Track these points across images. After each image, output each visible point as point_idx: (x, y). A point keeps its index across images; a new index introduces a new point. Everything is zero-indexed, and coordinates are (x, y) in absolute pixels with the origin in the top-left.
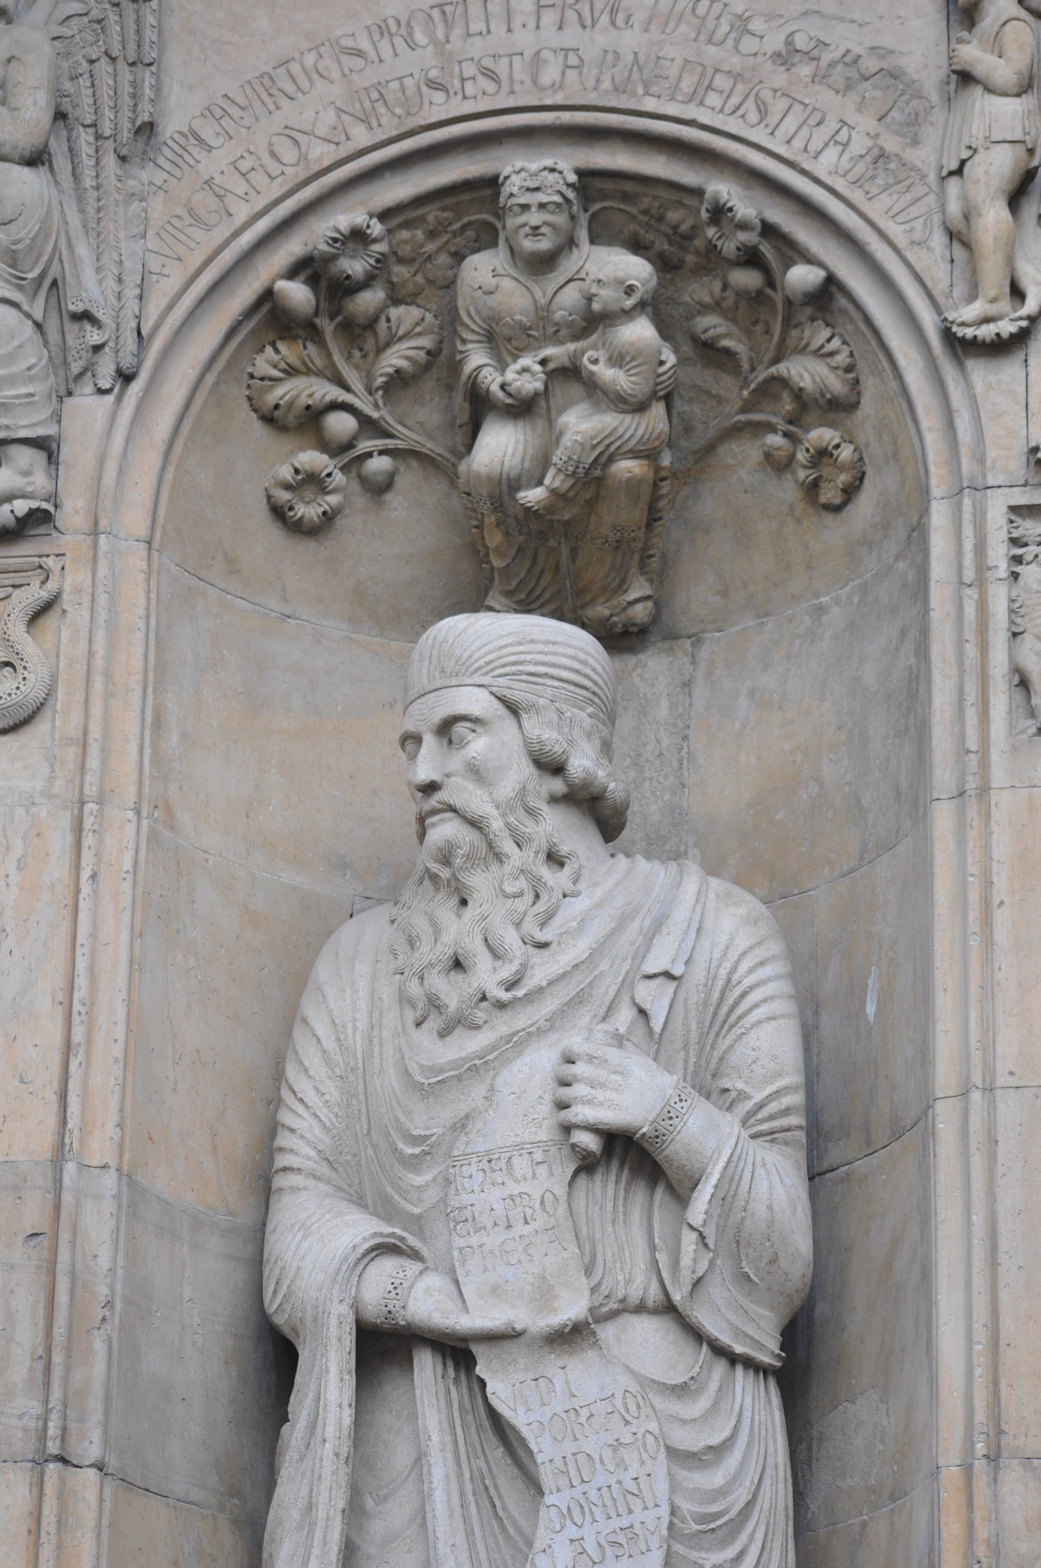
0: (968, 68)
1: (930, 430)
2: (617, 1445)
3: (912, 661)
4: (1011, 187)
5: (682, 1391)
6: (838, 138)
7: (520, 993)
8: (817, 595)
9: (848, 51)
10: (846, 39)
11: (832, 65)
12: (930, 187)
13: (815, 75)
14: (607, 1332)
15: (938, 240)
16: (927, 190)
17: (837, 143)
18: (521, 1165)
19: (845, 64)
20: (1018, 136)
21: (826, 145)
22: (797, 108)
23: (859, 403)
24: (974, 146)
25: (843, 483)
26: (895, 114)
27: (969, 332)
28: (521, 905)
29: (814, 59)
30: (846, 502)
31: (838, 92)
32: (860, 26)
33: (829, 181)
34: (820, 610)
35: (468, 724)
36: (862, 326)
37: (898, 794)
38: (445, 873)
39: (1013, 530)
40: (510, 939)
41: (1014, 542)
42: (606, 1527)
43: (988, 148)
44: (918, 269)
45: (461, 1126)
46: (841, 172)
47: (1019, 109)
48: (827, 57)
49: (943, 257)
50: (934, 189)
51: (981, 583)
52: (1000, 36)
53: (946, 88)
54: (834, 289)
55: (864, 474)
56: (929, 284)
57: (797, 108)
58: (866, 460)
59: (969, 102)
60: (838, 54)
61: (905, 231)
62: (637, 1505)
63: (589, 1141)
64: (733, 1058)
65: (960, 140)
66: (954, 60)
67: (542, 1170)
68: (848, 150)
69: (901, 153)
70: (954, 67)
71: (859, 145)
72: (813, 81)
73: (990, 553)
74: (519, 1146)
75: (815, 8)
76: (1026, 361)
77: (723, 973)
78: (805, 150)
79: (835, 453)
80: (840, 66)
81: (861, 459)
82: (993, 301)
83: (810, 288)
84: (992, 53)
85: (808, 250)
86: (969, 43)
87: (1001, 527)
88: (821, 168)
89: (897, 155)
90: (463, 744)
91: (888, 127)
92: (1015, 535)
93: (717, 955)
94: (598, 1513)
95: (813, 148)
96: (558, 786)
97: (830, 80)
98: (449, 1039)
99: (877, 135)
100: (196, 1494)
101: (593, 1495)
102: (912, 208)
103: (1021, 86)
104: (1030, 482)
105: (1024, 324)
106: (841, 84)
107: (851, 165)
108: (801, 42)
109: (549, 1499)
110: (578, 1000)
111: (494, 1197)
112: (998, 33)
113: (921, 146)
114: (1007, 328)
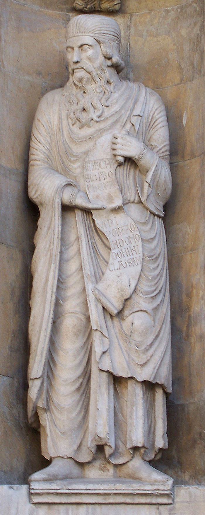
2: (129, 238)
3: (198, 32)
5: (145, 223)
7: (102, 119)
8: (167, 7)
14: (125, 207)
18: (103, 164)
28: (101, 95)
34: (168, 11)
35: (88, 46)
38: (80, 85)
40: (99, 105)
42: (127, 258)
45: (87, 153)
62: (134, 253)
63: (121, 159)
64: (154, 137)
67: (108, 166)
74: (103, 159)
77: (151, 114)
90: (86, 51)
93: (150, 110)
94: (125, 254)
96: (109, 63)
98: (82, 129)
100: (12, 244)
101: (124, 250)
109: (112, 251)
110: (117, 121)
111: (96, 172)
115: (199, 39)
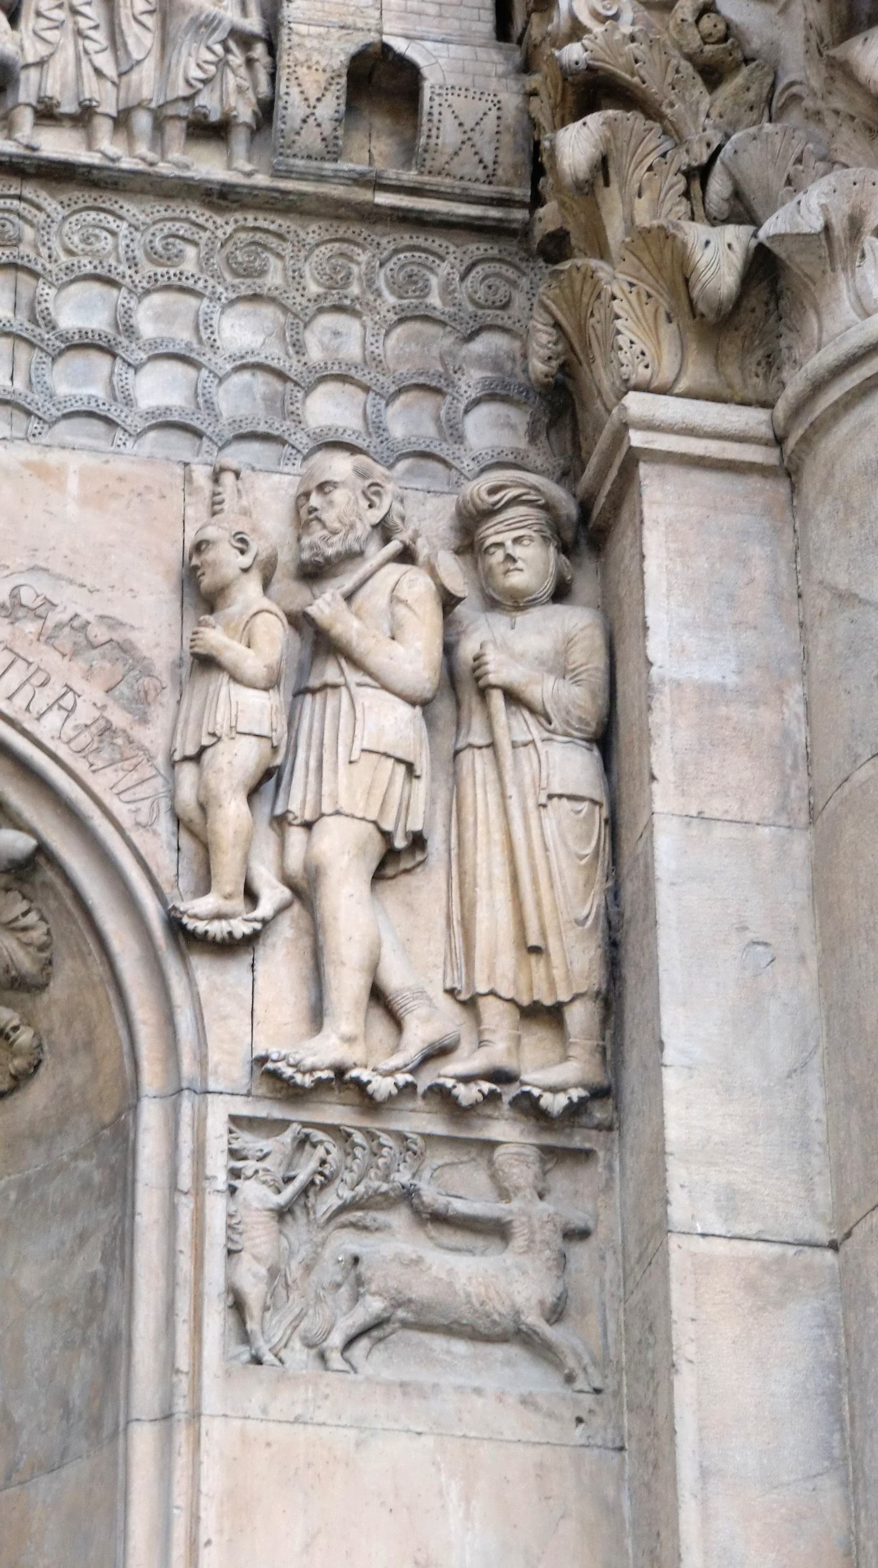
0: (214, 653)
1: (144, 1023)
4: (252, 782)
6: (62, 703)
9: (76, 616)
10: (76, 603)
11: (59, 626)
12: (156, 769)
13: (40, 634)
15: (165, 825)
16: (154, 772)
17: (61, 707)
19: (72, 628)
20: (266, 731)
21: (50, 708)
22: (20, 664)
23: (46, 985)
24: (218, 733)
25: (16, 1070)
26: (123, 688)
27: (201, 926)
29: (39, 617)
30: (12, 1090)
31: (64, 655)
32: (91, 592)
33: (51, 745)
36: (70, 903)
37: (67, 1412)
39: (233, 1141)
41: (234, 1154)
43: (233, 738)
44: (143, 852)
46: (65, 738)
47: (268, 704)
48: (54, 618)
49: (169, 845)
50: (162, 772)
51: (198, 1192)
52: (249, 626)
53: (178, 671)
54: (41, 860)
55: (40, 1061)
56: (154, 870)
57: (20, 664)
58: (46, 1048)
59: (211, 689)
60: (65, 617)
61: (129, 810)
65: (200, 726)
66: (197, 642)
68: (72, 717)
69: (128, 729)
70: (196, 650)
71: (85, 714)
72: (38, 640)
73: (209, 1161)
75: (43, 564)
76: (253, 966)
78: (28, 709)
79: (13, 1036)
80: (67, 630)
81: (40, 1046)
82: (228, 897)
83: (18, 856)
84: (240, 642)
85: (19, 815)
86: (214, 627)
87: (221, 1136)
88: (45, 730)
89: (124, 731)
91: (116, 700)
92: (236, 1145)
95: (36, 708)
97: (57, 643)
99: (104, 707)
102: (138, 789)
103: (270, 681)
104: (254, 1092)
105: (258, 926)
106: (68, 648)
107: (76, 733)
108: (26, 596)
112: (248, 622)
113: (150, 726)
114: (241, 928)
115: (100, 1293)
